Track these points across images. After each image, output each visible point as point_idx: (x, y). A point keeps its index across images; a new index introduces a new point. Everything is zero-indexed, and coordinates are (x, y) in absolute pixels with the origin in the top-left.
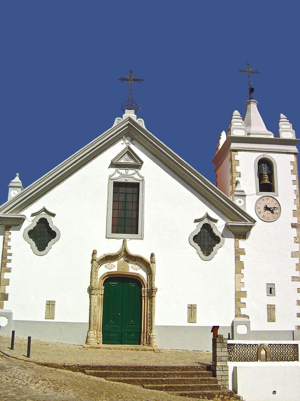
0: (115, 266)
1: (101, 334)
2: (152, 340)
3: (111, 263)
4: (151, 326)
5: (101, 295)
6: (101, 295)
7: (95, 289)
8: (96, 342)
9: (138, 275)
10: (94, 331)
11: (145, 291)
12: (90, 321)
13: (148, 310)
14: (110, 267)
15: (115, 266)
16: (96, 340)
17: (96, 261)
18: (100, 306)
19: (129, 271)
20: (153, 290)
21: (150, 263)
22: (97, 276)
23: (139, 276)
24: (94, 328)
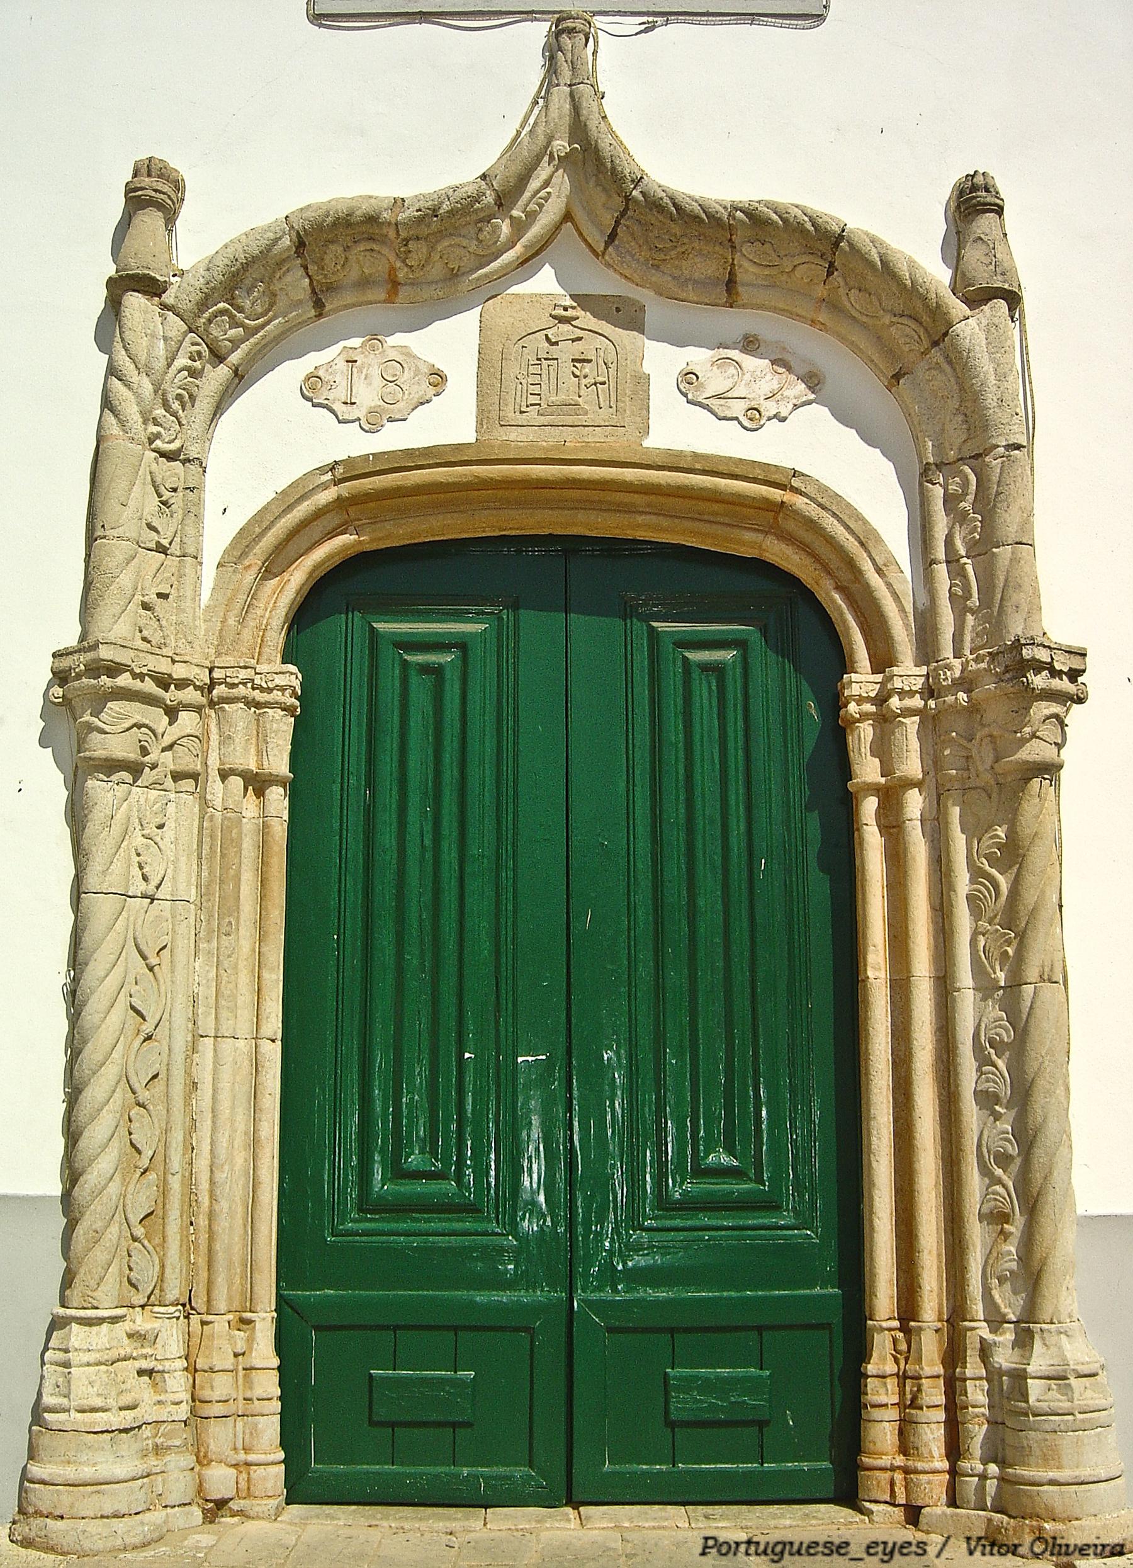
0: (438, 379)
1: (265, 1353)
2: (1051, 1458)
3: (391, 341)
4: (1015, 1228)
5: (257, 783)
6: (257, 783)
7: (149, 686)
8: (178, 1485)
9: (776, 494)
10: (141, 1321)
11: (895, 702)
12: (72, 1173)
13: (965, 977)
14: (367, 396)
15: (438, 379)
16: (179, 1462)
17: (169, 298)
18: (245, 939)
19: (647, 443)
20: (1039, 681)
21: (958, 307)
22: (194, 513)
23: (800, 502)
24: (147, 1275)
